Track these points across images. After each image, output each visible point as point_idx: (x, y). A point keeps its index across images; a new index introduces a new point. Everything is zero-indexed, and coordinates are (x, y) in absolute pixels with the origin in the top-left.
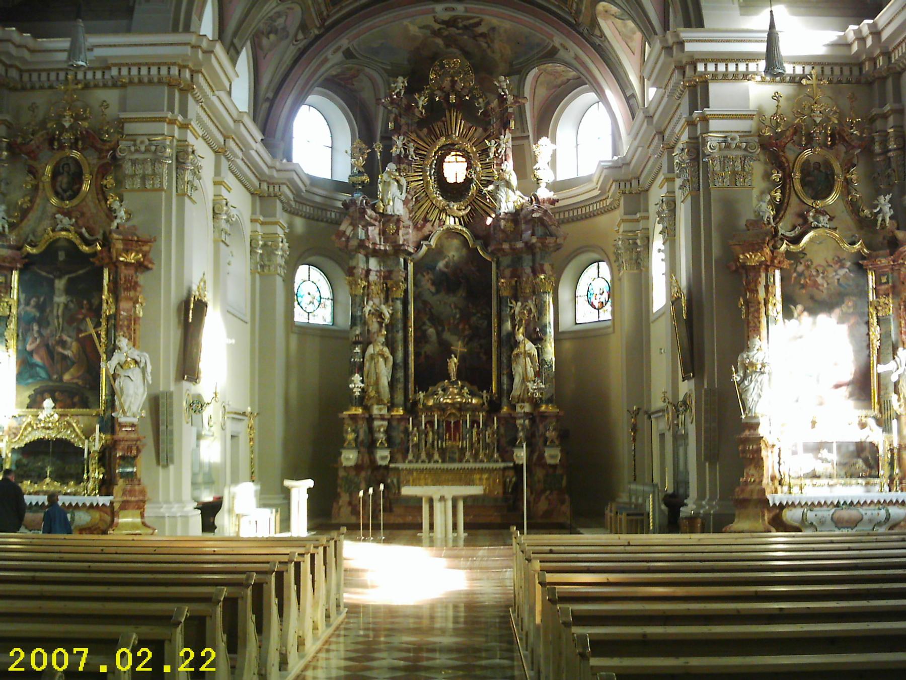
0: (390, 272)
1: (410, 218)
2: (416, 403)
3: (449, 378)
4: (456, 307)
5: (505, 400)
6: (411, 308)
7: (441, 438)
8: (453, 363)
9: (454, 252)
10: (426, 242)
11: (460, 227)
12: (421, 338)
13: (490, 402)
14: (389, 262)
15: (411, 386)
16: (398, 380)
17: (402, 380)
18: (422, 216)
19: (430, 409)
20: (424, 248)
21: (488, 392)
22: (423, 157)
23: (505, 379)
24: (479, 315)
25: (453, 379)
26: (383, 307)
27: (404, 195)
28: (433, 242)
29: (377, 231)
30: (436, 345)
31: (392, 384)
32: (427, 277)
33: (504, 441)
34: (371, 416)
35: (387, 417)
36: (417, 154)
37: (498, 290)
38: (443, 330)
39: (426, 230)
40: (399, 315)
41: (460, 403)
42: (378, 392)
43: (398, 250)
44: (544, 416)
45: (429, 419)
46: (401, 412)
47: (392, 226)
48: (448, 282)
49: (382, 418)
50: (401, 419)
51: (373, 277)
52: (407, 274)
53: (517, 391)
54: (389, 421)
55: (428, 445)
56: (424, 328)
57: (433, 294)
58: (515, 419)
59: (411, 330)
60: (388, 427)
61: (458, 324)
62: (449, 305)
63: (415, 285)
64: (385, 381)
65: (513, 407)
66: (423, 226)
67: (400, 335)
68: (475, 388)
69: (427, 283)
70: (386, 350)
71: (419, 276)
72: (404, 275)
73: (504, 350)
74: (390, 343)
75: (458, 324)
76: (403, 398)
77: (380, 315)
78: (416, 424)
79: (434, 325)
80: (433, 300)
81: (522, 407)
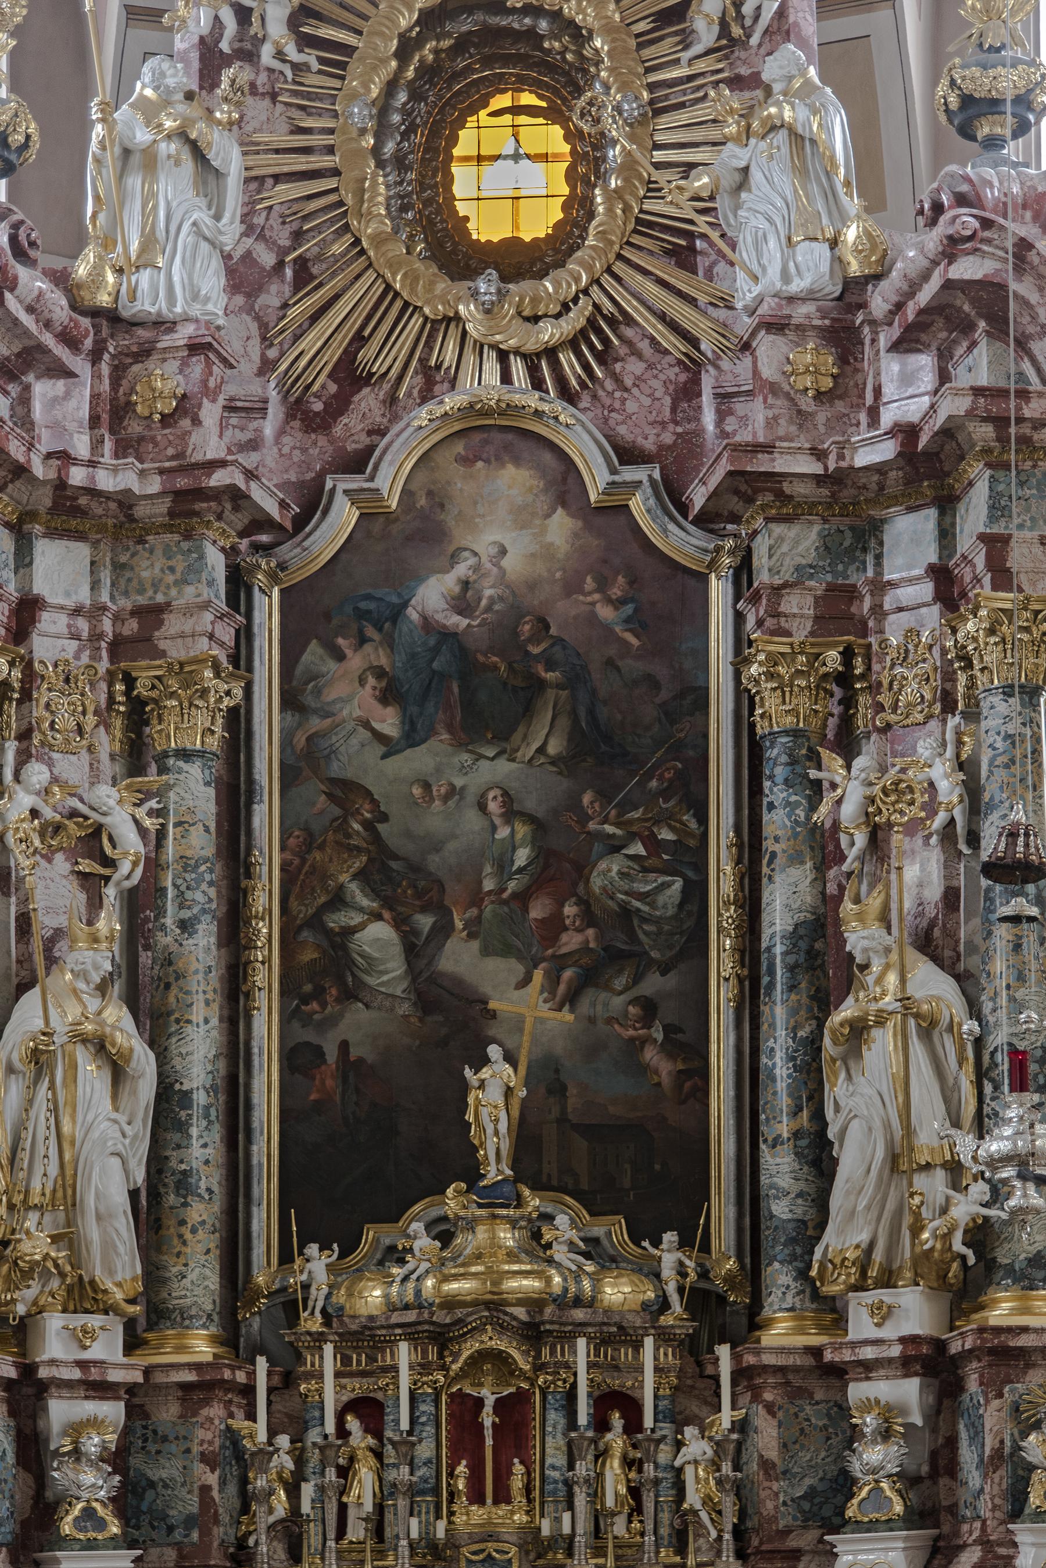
0: (152, 615)
1: (267, 366)
2: (290, 1305)
3: (471, 1173)
4: (510, 814)
5: (780, 1279)
6: (266, 819)
7: (433, 1496)
8: (493, 1094)
9: (507, 541)
10: (355, 482)
11: (532, 400)
12: (321, 974)
13: (702, 1300)
14: (149, 567)
15: (263, 1221)
16: (184, 1183)
17: (210, 1179)
18: (334, 354)
19: (365, 1341)
20: (343, 517)
21: (685, 1243)
22: (338, 58)
23: (780, 1168)
24: (638, 848)
25: (494, 1172)
26: (106, 795)
27: (230, 231)
28: (390, 479)
29: (79, 406)
30: (404, 1009)
31: (153, 1211)
32: (356, 662)
33: (775, 1500)
34: (28, 1370)
35: (124, 1372)
36: (306, 42)
37: (746, 701)
38: (443, 930)
39: (352, 428)
40: (201, 843)
41: (534, 1303)
42: (66, 1238)
43: (190, 503)
44: (1007, 1356)
45: (356, 1387)
46: (202, 1347)
47: (165, 379)
48: (471, 686)
49: (100, 1389)
50: (200, 1390)
51: (52, 642)
52: (245, 635)
53: (843, 1237)
54: (137, 1399)
55: (356, 1531)
56: (336, 920)
57: (390, 747)
58: (838, 1374)
59: (266, 932)
60: (126, 1432)
61: (523, 898)
62: (469, 798)
63: (291, 700)
64: (110, 1184)
65: (832, 1313)
66: (338, 406)
67: (201, 951)
68: (613, 1230)
69: (351, 693)
70: (118, 1020)
71: (313, 653)
72: (226, 633)
73: (778, 1011)
74: (147, 991)
75: (523, 898)
76: (213, 1282)
77: (94, 842)
78: (294, 1422)
79: (393, 907)
80: (386, 775)
81: (883, 1314)
